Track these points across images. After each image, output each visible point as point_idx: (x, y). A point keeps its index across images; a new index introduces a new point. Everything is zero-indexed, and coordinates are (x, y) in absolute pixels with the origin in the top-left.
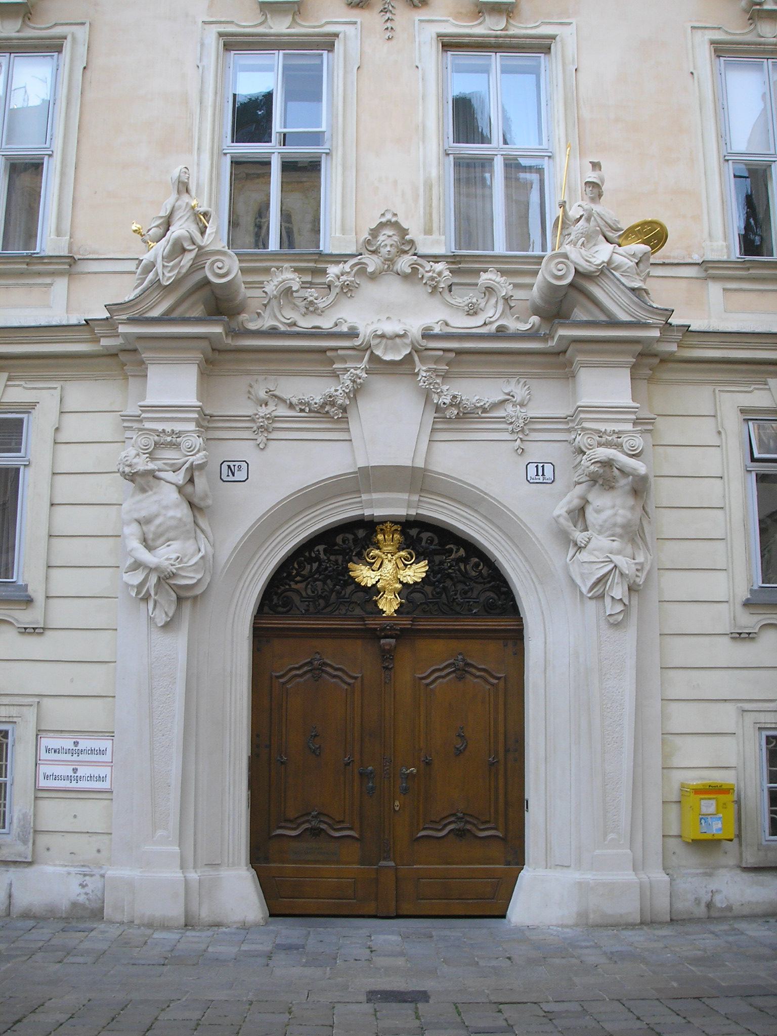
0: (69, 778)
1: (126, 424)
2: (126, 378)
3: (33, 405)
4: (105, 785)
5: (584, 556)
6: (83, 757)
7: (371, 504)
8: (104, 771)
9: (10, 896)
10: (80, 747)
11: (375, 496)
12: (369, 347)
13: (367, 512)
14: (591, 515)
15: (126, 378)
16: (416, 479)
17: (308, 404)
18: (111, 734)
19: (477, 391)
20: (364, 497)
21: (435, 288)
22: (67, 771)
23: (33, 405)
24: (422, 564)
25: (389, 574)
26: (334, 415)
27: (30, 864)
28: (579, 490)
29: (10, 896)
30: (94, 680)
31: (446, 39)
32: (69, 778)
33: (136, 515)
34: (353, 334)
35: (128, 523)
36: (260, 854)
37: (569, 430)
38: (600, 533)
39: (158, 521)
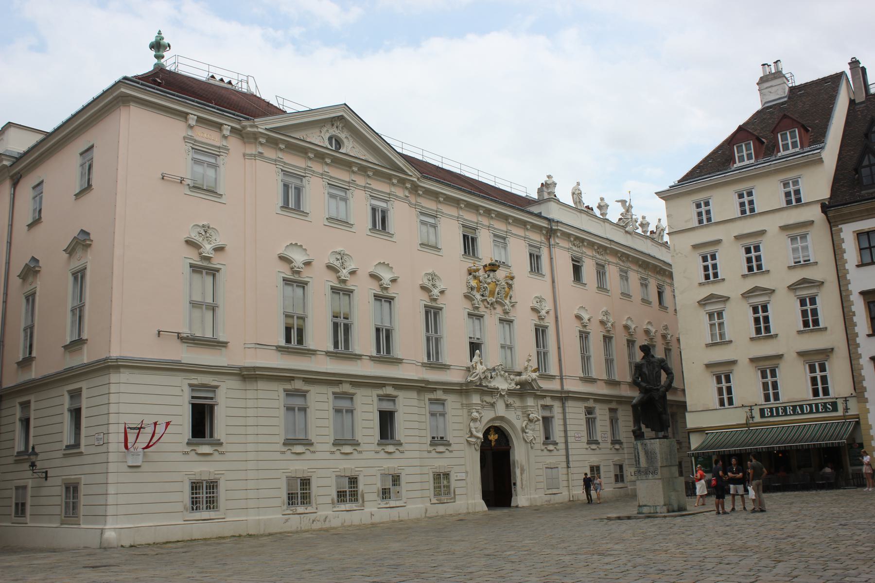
16: (502, 418)
19: (510, 400)
25: (493, 437)
26: (493, 405)
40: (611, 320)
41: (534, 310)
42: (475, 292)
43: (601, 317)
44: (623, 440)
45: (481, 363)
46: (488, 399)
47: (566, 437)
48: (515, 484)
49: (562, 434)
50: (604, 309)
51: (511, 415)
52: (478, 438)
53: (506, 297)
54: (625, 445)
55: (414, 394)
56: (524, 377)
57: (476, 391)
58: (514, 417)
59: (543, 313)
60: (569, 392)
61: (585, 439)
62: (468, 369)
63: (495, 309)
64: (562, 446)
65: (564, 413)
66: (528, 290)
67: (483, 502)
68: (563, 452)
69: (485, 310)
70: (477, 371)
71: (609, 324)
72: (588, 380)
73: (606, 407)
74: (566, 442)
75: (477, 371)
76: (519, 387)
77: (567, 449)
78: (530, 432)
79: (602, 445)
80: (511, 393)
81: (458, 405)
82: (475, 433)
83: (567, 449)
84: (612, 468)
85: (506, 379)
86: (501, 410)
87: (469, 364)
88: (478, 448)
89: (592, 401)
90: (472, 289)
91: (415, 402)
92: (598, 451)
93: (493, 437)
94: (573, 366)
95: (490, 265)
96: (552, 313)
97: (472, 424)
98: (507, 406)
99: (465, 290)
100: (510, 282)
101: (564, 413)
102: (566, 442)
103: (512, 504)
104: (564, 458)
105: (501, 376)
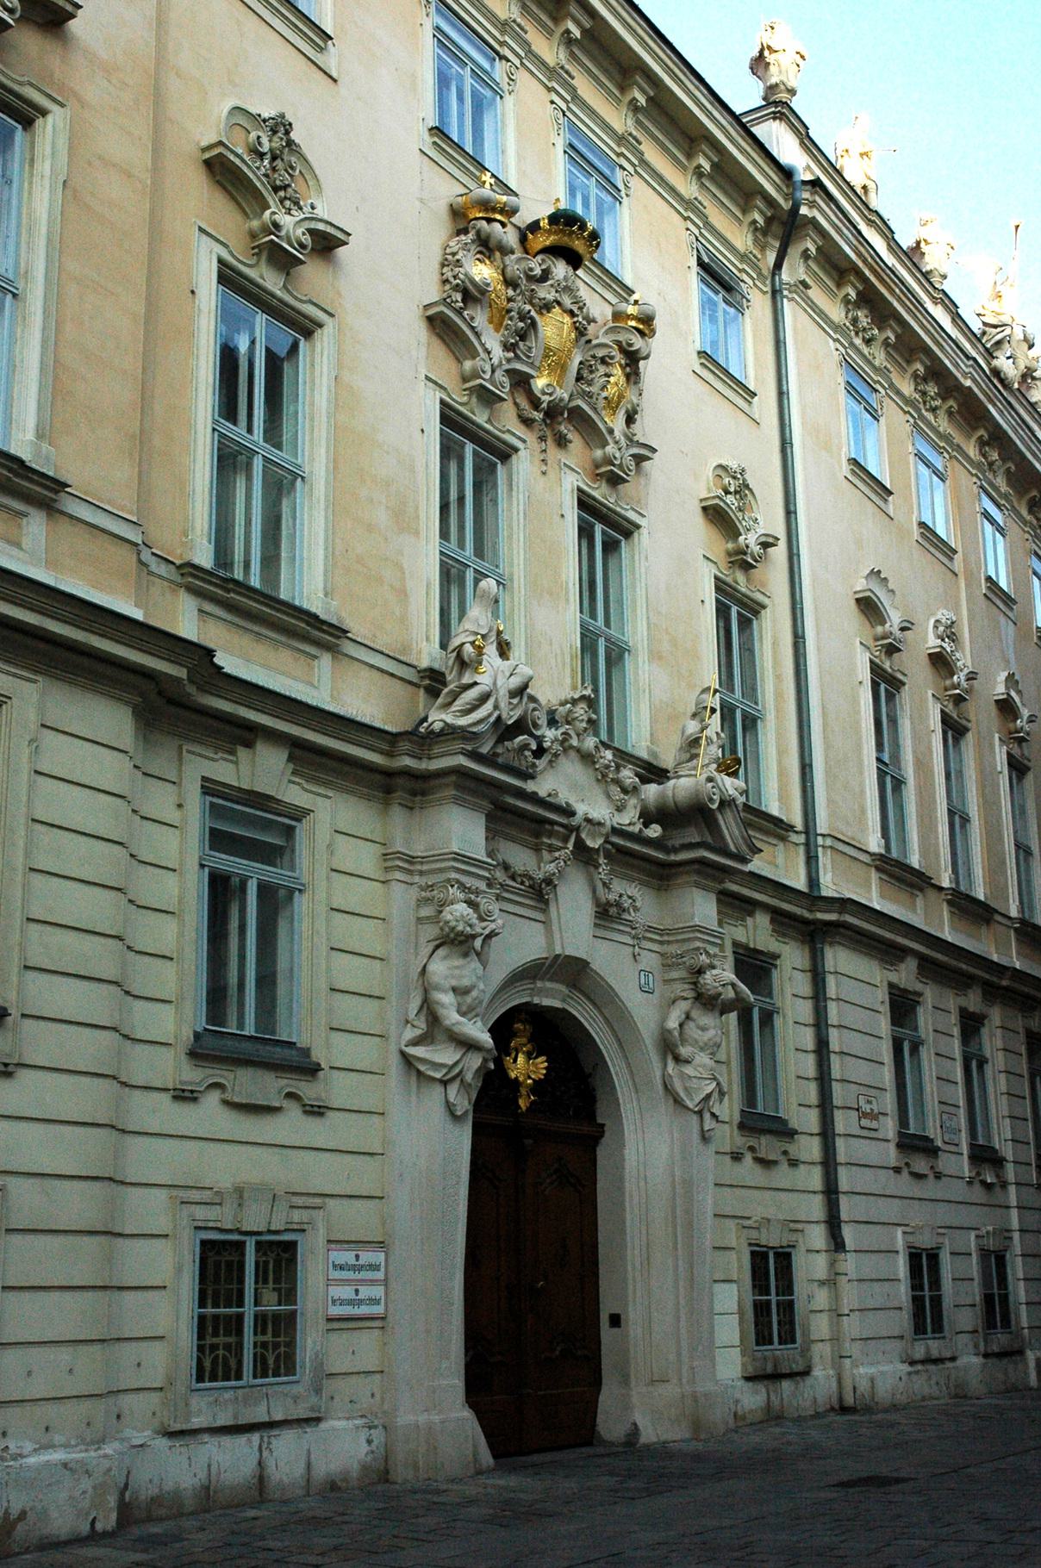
0: (351, 1302)
1: (390, 864)
2: (387, 804)
3: (306, 812)
4: (378, 1310)
5: (689, 1070)
6: (363, 1275)
7: (540, 992)
8: (378, 1292)
9: (309, 1465)
10: (361, 1262)
11: (548, 985)
12: (577, 829)
13: (536, 1000)
14: (692, 1030)
15: (387, 804)
17: (531, 878)
18: (381, 1245)
20: (539, 984)
21: (604, 776)
22: (346, 1292)
23: (306, 812)
24: (543, 1058)
26: (540, 893)
27: (318, 1420)
28: (684, 1006)
29: (309, 1465)
30: (364, 1177)
31: (585, 499)
32: (351, 1302)
33: (454, 983)
34: (569, 812)
35: (445, 991)
36: (477, 1388)
37: (661, 943)
38: (702, 1049)
39: (474, 993)
40: (964, 660)
41: (716, 515)
42: (480, 318)
43: (932, 643)
44: (1008, 1151)
45: (504, 649)
46: (521, 858)
47: (825, 1106)
48: (615, 1320)
49: (812, 1093)
50: (944, 615)
51: (613, 961)
52: (469, 1045)
53: (612, 405)
54: (1010, 1172)
55: (110, 719)
56: (682, 787)
57: (469, 786)
58: (637, 969)
59: (750, 540)
60: (844, 904)
61: (889, 1127)
62: (433, 682)
63: (562, 442)
64: (810, 1148)
65: (819, 996)
66: (687, 430)
67: (467, 1414)
68: (815, 1179)
69: (520, 430)
70: (484, 680)
71: (960, 678)
72: (894, 870)
73: (952, 1002)
74: (827, 1134)
75: (484, 680)
76: (655, 831)
77: (829, 1163)
78: (703, 1059)
79: (946, 1163)
80: (625, 854)
81: (365, 858)
82: (452, 1017)
83: (829, 1163)
84: (974, 1266)
85: (603, 778)
86: (572, 925)
87: (428, 653)
88: (463, 1104)
89: (911, 964)
90: (471, 294)
91: (110, 770)
92: (931, 1188)
93: (525, 1068)
94: (850, 806)
95: (554, 219)
96: (779, 553)
97: (442, 968)
98: (607, 914)
99: (433, 293)
100: (638, 343)
101: (819, 996)
102: (827, 1134)
103: (610, 1425)
104: (815, 1207)
105: (587, 758)
